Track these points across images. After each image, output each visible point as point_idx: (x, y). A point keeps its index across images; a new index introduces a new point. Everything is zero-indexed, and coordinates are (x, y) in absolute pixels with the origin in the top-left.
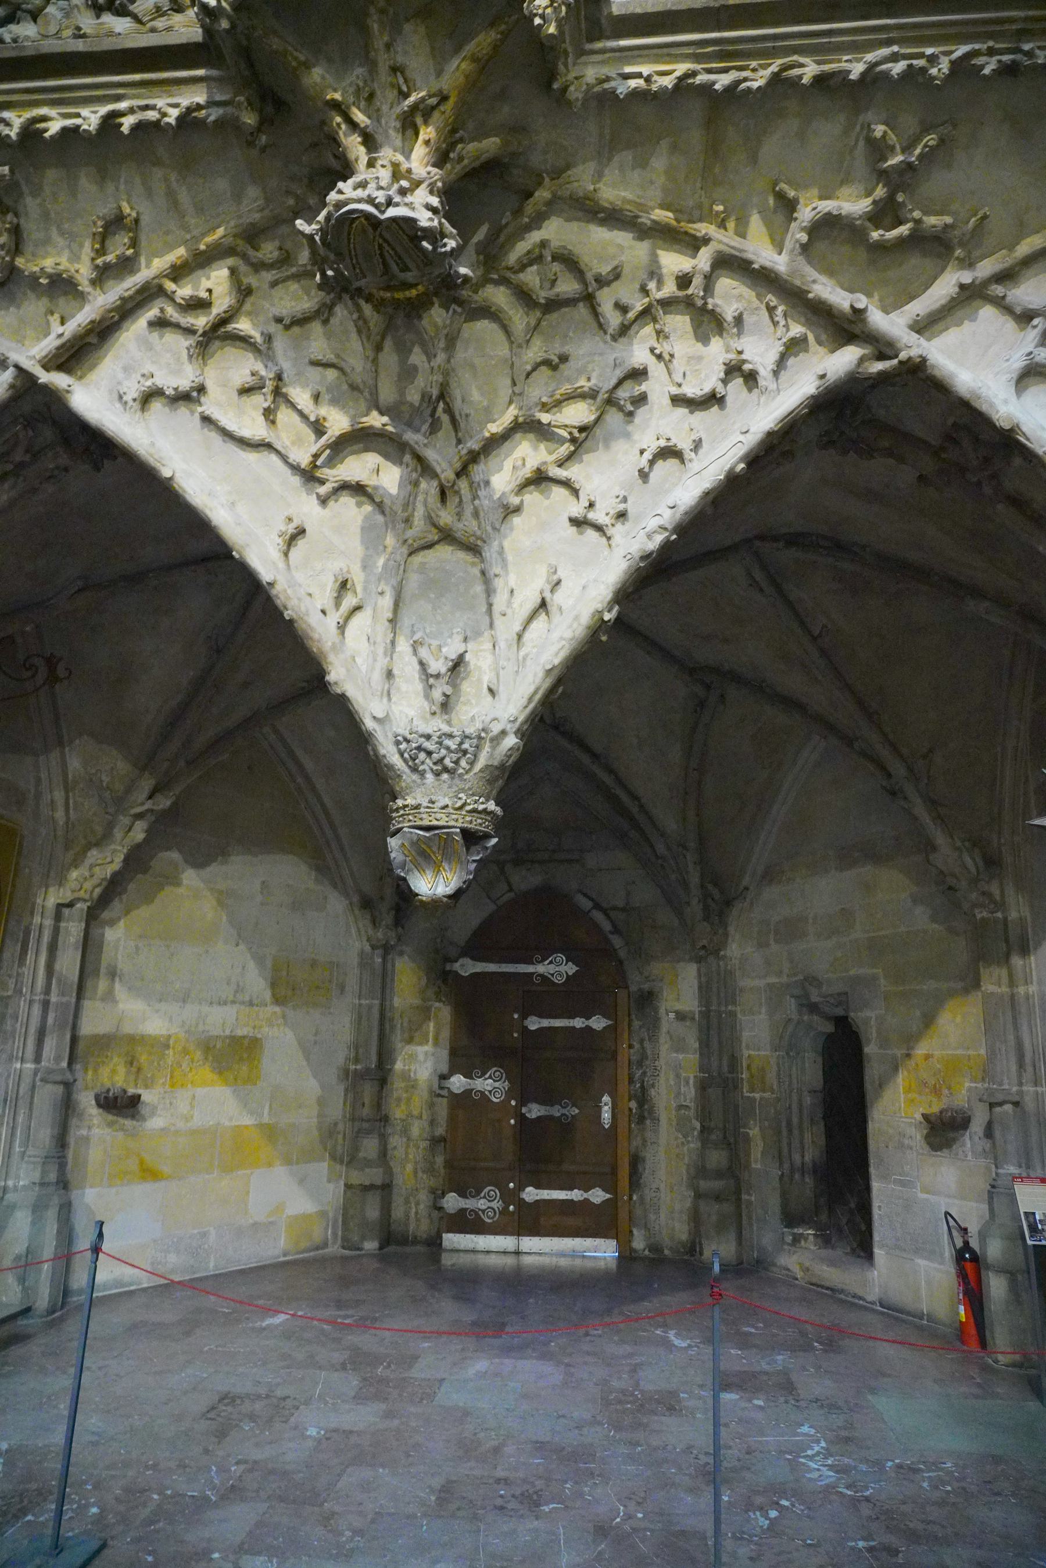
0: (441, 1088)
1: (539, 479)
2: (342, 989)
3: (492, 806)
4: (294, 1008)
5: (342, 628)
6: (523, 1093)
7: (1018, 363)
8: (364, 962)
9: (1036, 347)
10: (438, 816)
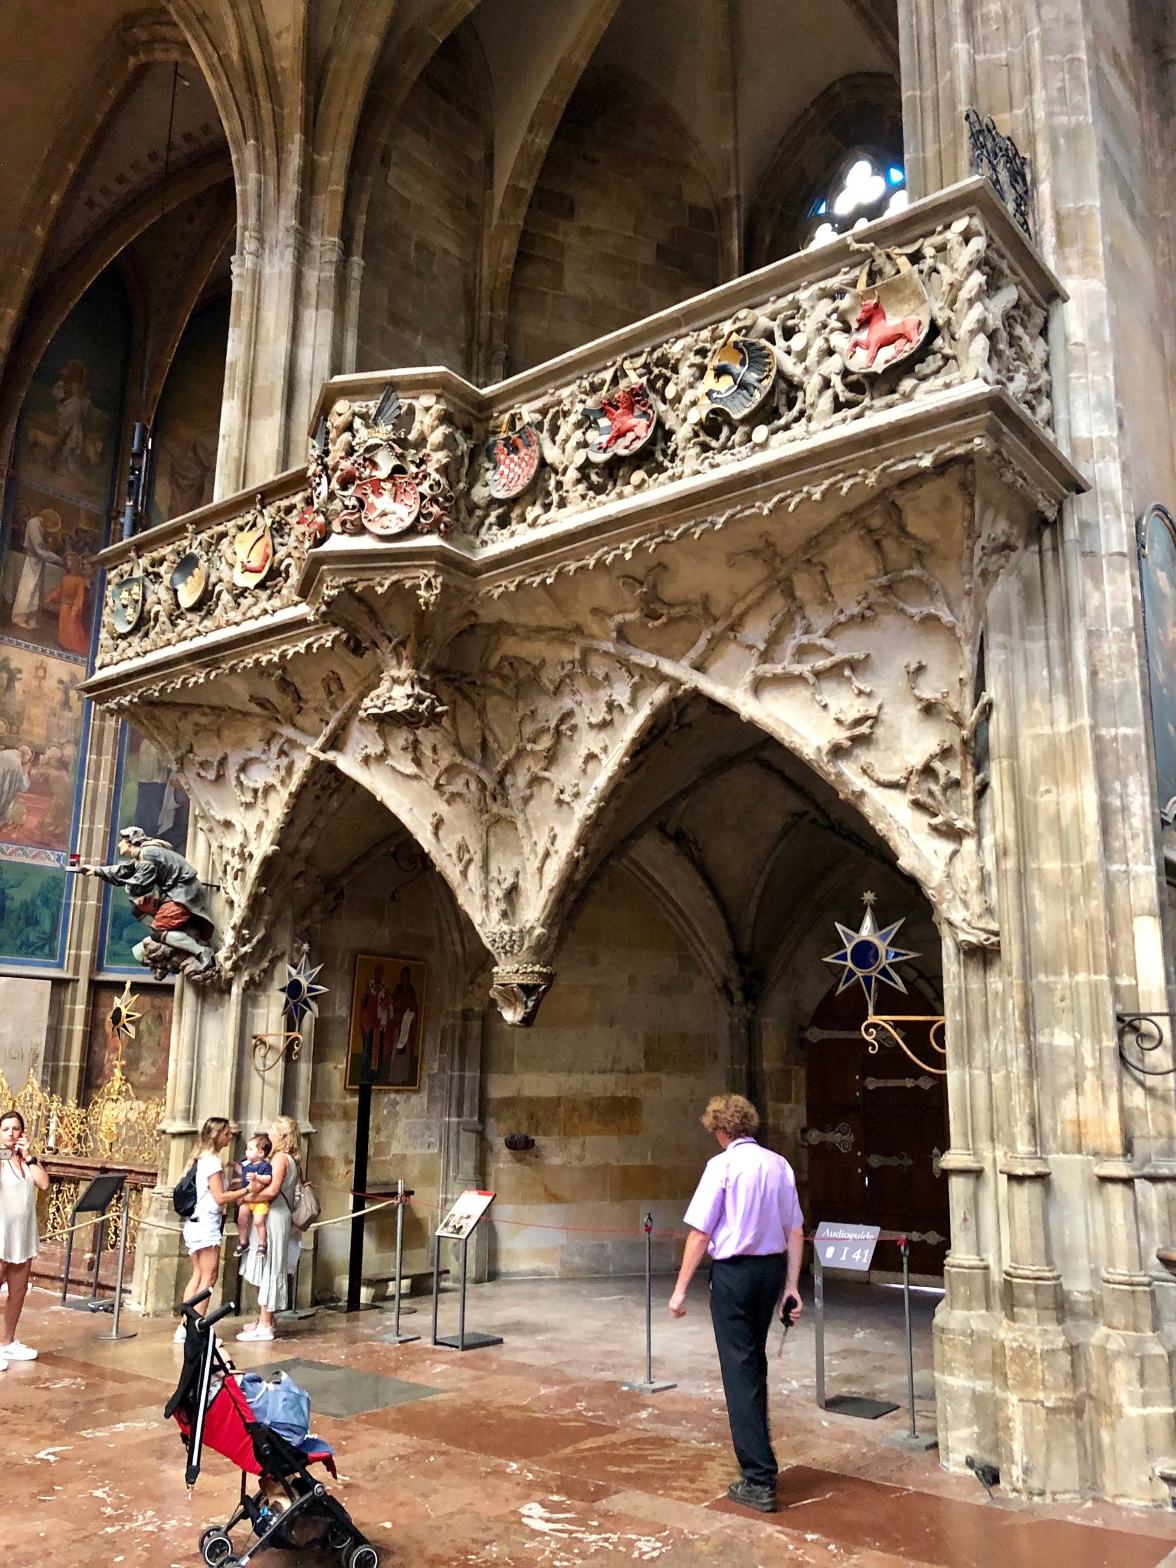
0: (803, 1139)
1: (536, 781)
2: (715, 1056)
3: (537, 968)
4: (668, 1073)
5: (464, 873)
6: (868, 1143)
7: (748, 678)
8: (733, 1035)
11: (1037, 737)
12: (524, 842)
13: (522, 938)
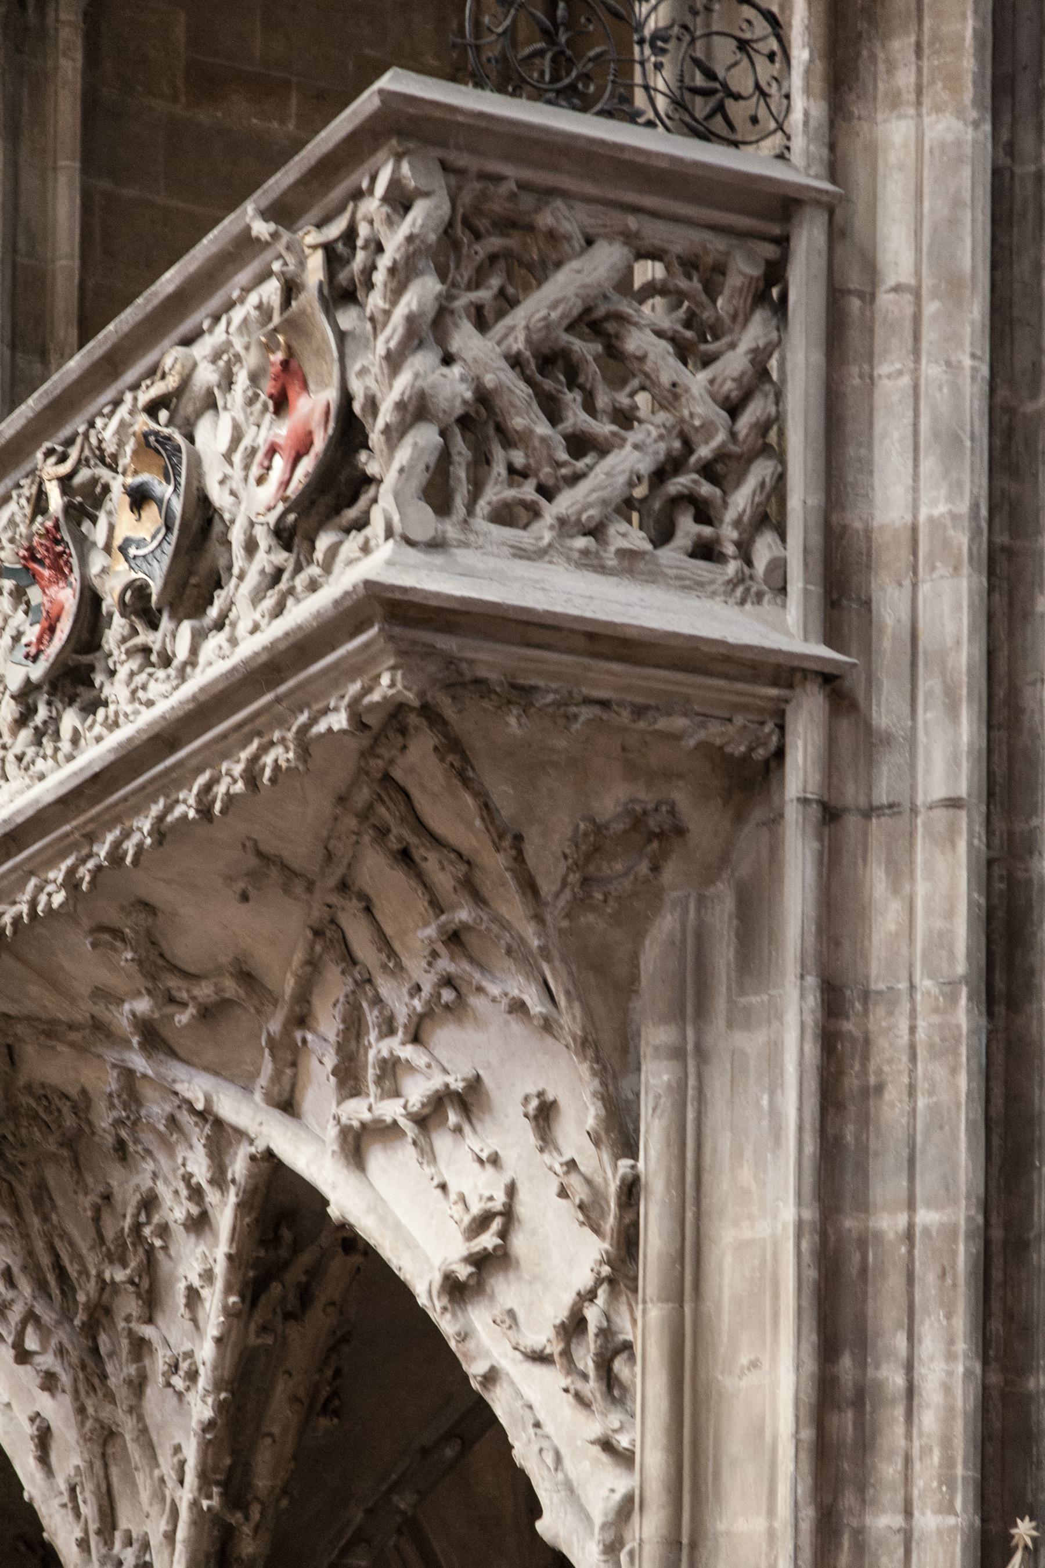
7: (332, 1132)
9: (339, 1104)
11: (741, 1246)
12: (140, 1478)
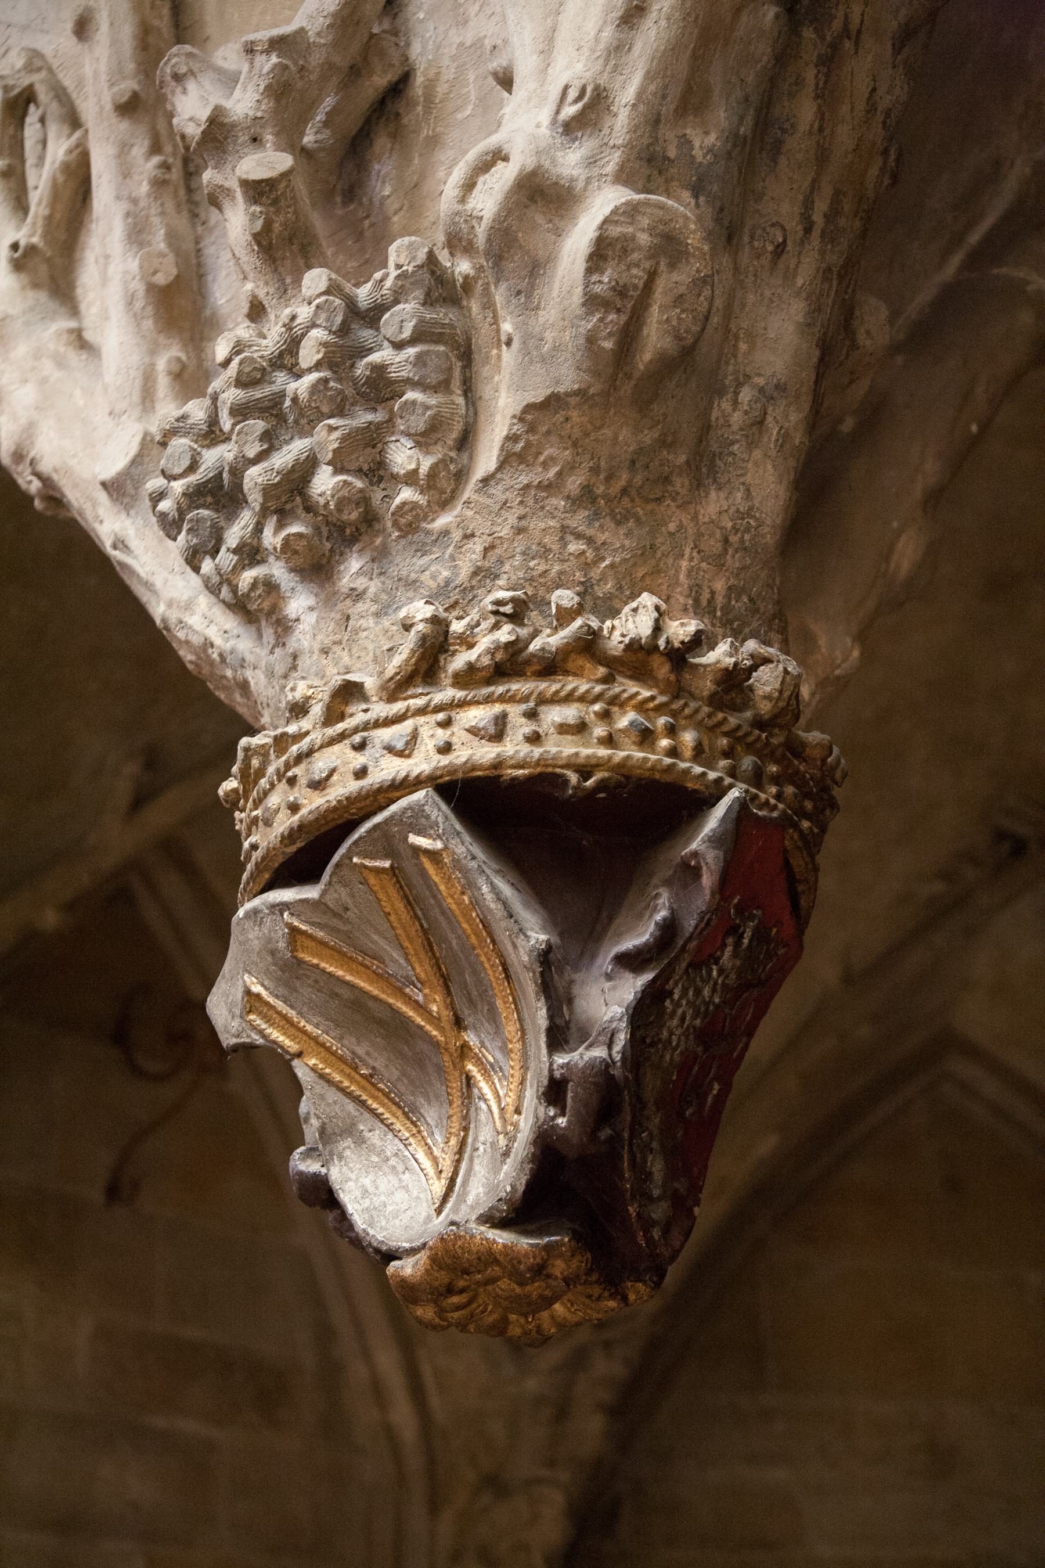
10: (321, 764)
13: (460, 361)
